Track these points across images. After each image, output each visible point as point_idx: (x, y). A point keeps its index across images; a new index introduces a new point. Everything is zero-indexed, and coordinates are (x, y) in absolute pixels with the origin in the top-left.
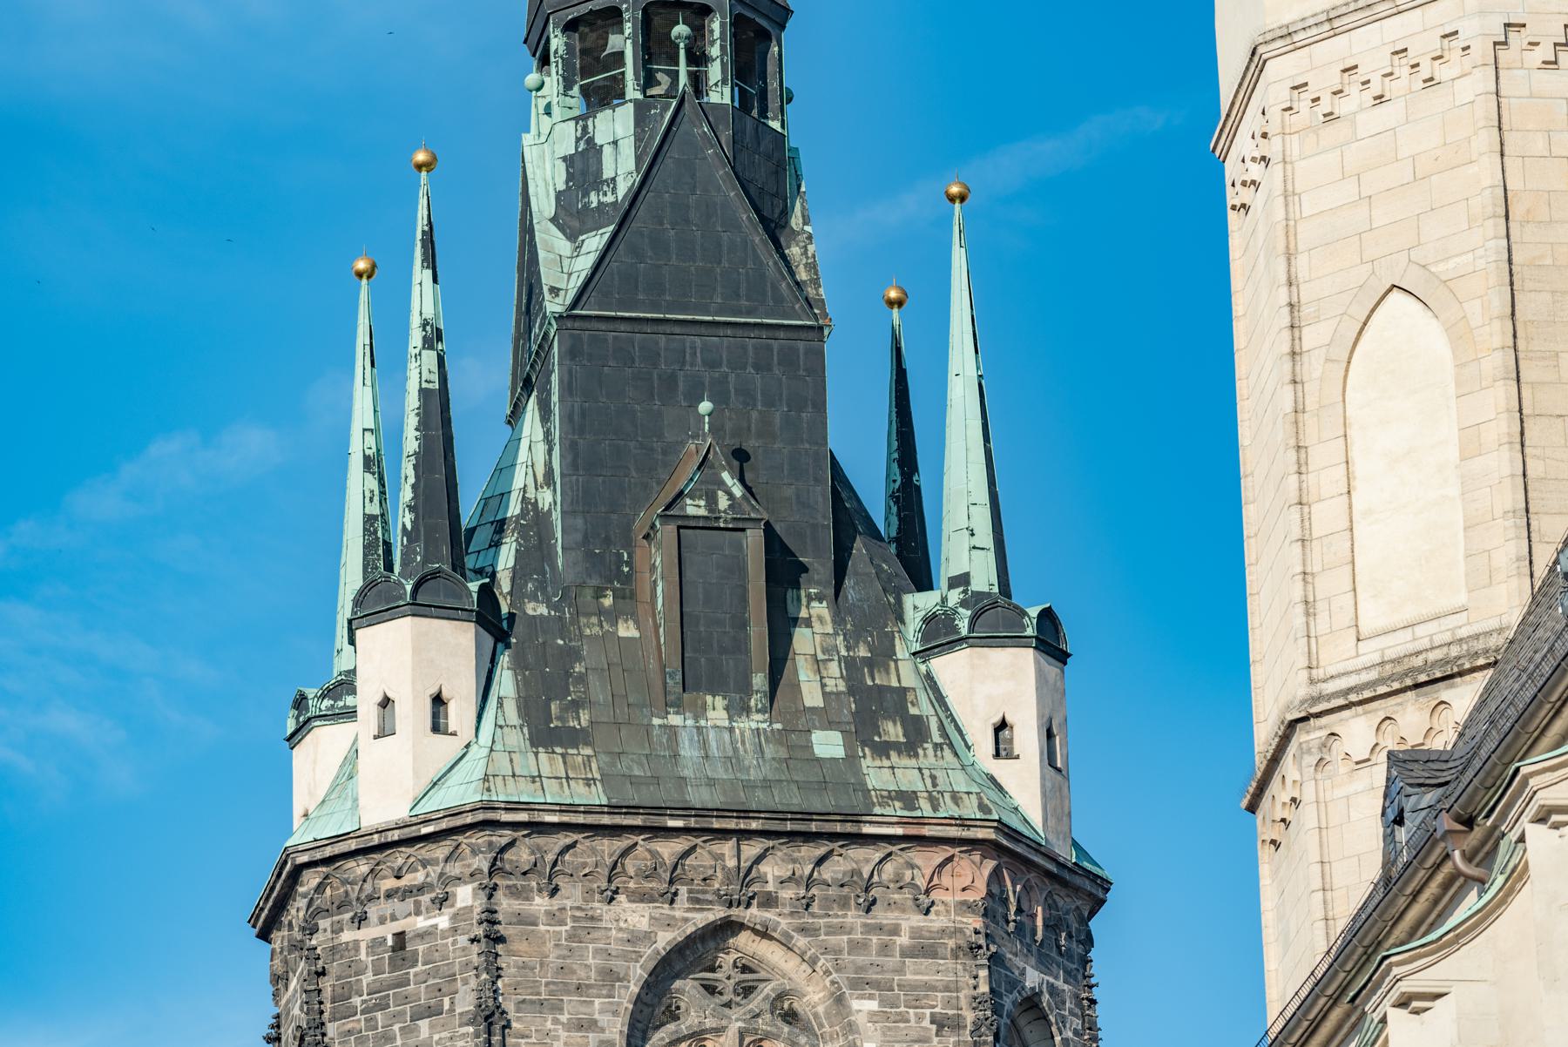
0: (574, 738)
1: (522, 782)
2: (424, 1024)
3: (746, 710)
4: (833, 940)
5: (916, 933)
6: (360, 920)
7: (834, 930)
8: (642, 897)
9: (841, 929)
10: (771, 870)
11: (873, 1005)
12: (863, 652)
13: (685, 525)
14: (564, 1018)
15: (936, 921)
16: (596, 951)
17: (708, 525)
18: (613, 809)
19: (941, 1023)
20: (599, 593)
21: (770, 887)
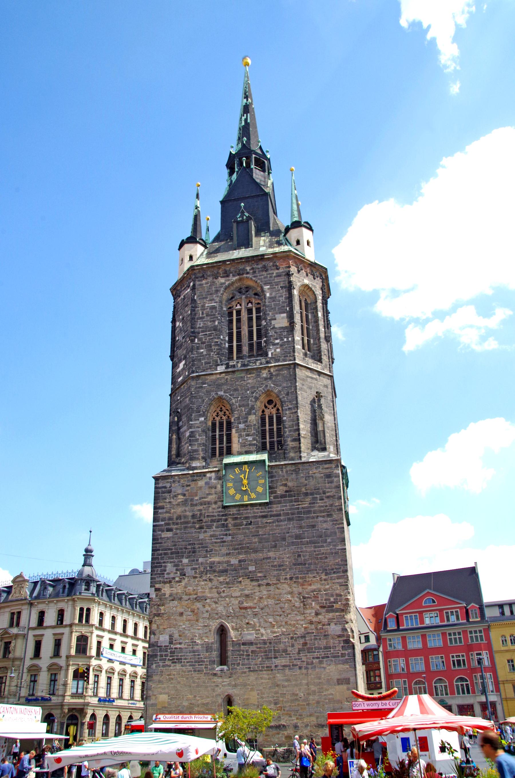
4: (260, 277)
6: (180, 296)
7: (260, 276)
9: (262, 275)
10: (248, 268)
11: (269, 287)
14: (208, 299)
15: (281, 270)
17: (242, 221)
19: (282, 287)
20: (227, 240)
21: (248, 271)
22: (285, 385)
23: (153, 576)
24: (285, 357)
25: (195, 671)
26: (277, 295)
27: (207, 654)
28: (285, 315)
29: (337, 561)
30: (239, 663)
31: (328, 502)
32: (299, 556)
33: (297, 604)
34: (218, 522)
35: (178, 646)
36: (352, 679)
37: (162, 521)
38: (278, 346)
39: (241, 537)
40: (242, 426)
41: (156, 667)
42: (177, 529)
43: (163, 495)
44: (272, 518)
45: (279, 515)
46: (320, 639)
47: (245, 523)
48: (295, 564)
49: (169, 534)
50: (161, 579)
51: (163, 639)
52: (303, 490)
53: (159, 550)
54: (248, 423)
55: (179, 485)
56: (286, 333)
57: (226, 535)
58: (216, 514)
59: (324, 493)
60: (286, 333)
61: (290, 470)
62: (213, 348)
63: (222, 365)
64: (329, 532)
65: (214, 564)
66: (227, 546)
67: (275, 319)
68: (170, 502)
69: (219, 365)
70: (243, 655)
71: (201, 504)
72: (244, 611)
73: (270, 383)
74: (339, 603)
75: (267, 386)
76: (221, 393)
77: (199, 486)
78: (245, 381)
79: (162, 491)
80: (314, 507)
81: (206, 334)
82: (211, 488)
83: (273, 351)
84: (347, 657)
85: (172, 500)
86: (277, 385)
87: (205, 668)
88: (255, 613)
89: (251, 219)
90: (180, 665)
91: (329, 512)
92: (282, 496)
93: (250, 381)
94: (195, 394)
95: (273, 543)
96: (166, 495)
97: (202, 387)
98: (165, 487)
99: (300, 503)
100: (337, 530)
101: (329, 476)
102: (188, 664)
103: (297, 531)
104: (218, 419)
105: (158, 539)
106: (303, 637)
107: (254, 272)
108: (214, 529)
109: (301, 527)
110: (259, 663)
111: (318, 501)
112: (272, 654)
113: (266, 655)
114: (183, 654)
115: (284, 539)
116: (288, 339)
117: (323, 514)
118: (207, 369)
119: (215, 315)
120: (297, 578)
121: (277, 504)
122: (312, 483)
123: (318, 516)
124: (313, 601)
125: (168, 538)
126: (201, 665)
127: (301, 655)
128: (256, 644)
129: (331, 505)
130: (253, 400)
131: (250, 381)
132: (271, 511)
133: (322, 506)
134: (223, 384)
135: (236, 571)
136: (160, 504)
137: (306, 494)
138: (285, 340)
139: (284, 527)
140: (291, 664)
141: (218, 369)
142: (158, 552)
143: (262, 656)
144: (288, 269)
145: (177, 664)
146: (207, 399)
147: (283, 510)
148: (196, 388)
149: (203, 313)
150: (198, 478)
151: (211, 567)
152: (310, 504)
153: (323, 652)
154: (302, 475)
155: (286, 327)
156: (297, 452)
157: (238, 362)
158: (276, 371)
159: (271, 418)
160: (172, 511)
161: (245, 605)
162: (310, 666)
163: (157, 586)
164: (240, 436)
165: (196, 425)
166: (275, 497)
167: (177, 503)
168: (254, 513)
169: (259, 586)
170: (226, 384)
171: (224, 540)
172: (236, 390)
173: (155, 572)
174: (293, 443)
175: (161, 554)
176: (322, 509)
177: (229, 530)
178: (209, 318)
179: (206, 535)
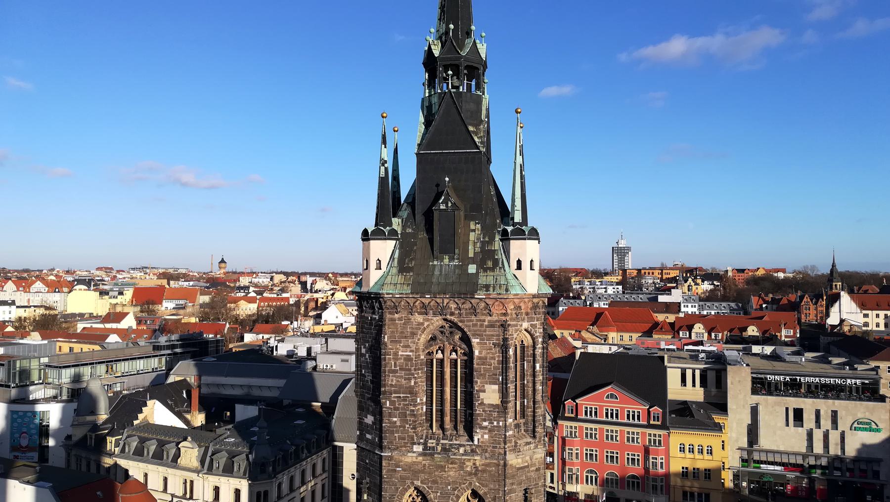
0: (409, 270)
1: (392, 287)
5: (489, 321)
7: (468, 321)
8: (420, 313)
9: (471, 321)
10: (453, 306)
11: (478, 340)
12: (487, 239)
22: (492, 486)
24: (494, 447)
28: (496, 387)
63: (419, 444)
67: (484, 391)
69: (414, 444)
75: (470, 484)
86: (483, 485)
89: (458, 209)
93: (451, 473)
97: (395, 471)
107: (460, 314)
116: (498, 423)
119: (410, 370)
131: (451, 473)
138: (495, 423)
141: (415, 450)
144: (504, 318)
148: (388, 471)
149: (395, 364)
170: (423, 472)
172: (435, 482)
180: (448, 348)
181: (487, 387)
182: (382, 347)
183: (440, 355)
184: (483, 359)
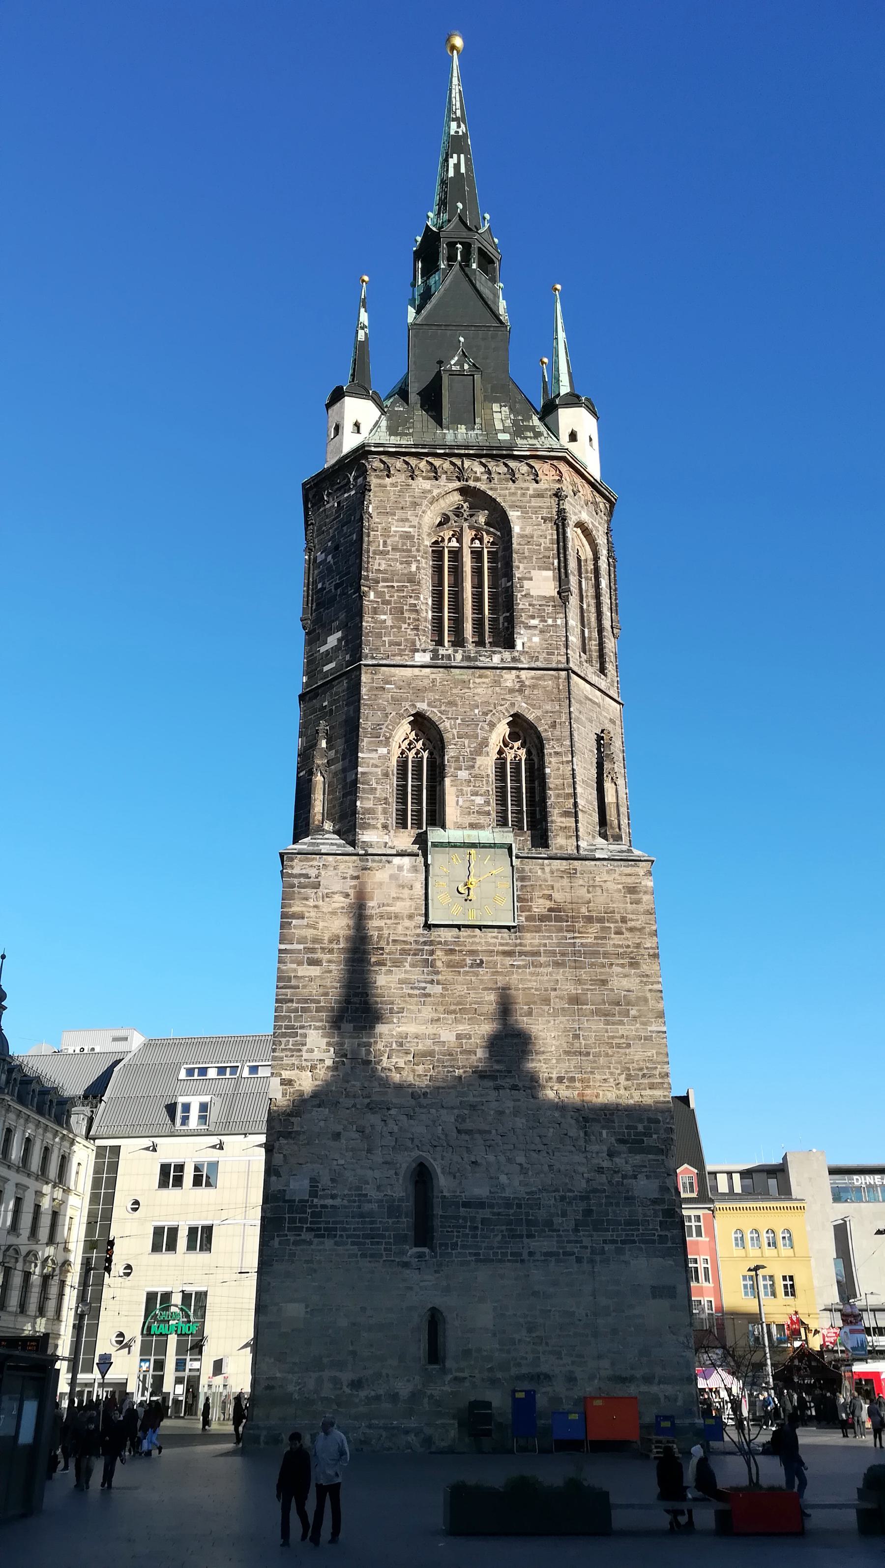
0: (406, 435)
2: (345, 528)
3: (474, 429)
5: (535, 490)
11: (519, 513)
13: (452, 374)
14: (396, 518)
15: (542, 485)
16: (409, 496)
17: (461, 374)
18: (416, 446)
19: (545, 520)
21: (478, 475)
22: (548, 707)
23: (275, 1054)
25: (364, 1256)
26: (536, 533)
27: (390, 1221)
28: (550, 574)
29: (649, 1054)
30: (456, 1244)
31: (630, 939)
32: (576, 1037)
33: (573, 1132)
34: (415, 955)
35: (329, 1202)
36: (681, 1288)
37: (299, 943)
38: (537, 632)
39: (460, 989)
40: (463, 774)
41: (280, 1244)
42: (329, 961)
43: (303, 890)
44: (523, 957)
45: (537, 954)
46: (618, 1205)
47: (469, 962)
48: (567, 1053)
49: (314, 971)
50: (294, 1060)
51: (298, 1187)
52: (584, 910)
53: (292, 1001)
54: (476, 771)
55: (337, 875)
56: (550, 608)
57: (432, 982)
58: (412, 939)
59: (624, 920)
60: (550, 608)
61: (558, 870)
62: (406, 615)
63: (424, 651)
64: (632, 996)
65: (406, 1038)
66: (434, 1004)
67: (531, 579)
68: (316, 907)
69: (417, 651)
70: (465, 1227)
71: (382, 917)
72: (467, 1137)
73: (519, 699)
74: (655, 1136)
76: (422, 706)
77: (377, 880)
78: (470, 688)
79: (300, 883)
80: (603, 945)
81: (393, 587)
82: (403, 887)
83: (526, 640)
84: (669, 1245)
85: (320, 903)
86: (533, 706)
87: (385, 1249)
88: (488, 1143)
90: (333, 1241)
91: (632, 958)
92: (543, 918)
93: (479, 690)
94: (368, 700)
95: (526, 1007)
96: (309, 891)
98: (307, 876)
99: (576, 935)
100: (649, 995)
101: (632, 890)
102: (350, 1240)
103: (572, 989)
104: (411, 755)
105: (289, 979)
106: (585, 1198)
107: (490, 480)
108: (408, 968)
109: (579, 981)
110: (496, 1245)
111: (613, 936)
112: (523, 1229)
113: (511, 1230)
114: (338, 1219)
115: (547, 1001)
116: (555, 619)
117: (622, 961)
118: (394, 655)
119: (410, 551)
120: (572, 1080)
121: (532, 932)
122: (600, 901)
123: (612, 964)
124: (603, 1127)
125: (311, 979)
126: (378, 1243)
127: (581, 1233)
128: (491, 1206)
129: (638, 946)
130: (487, 728)
131: (479, 690)
132: (521, 945)
133: (621, 946)
134: (426, 689)
135: (452, 1055)
136: (295, 909)
137: (589, 919)
138: (550, 621)
139: (546, 978)
140: (561, 1251)
142: (289, 1005)
143: (502, 1231)
145: (326, 1240)
146: (394, 713)
147: (545, 945)
148: (371, 689)
149: (385, 543)
150: (374, 864)
151: (401, 1045)
152: (596, 938)
153: (623, 1230)
154: (581, 882)
155: (552, 598)
156: (571, 836)
157: (456, 652)
158: (532, 678)
159: (517, 766)
160: (321, 925)
161: (468, 1125)
162: (598, 1258)
163: (286, 1074)
164: (460, 793)
165: (372, 761)
166: (528, 919)
167: (330, 910)
168: (489, 944)
169: (497, 1088)
171: (427, 991)
172: (452, 704)
173: (283, 1046)
174: (563, 819)
175: (296, 1010)
176: (621, 950)
177: (437, 973)
178: (398, 555)
179: (389, 978)
180: (468, 535)
181: (535, 573)
182: (366, 516)
183: (454, 543)
184: (528, 539)
